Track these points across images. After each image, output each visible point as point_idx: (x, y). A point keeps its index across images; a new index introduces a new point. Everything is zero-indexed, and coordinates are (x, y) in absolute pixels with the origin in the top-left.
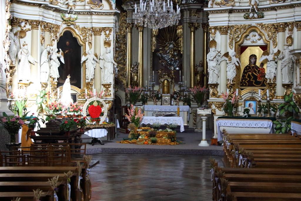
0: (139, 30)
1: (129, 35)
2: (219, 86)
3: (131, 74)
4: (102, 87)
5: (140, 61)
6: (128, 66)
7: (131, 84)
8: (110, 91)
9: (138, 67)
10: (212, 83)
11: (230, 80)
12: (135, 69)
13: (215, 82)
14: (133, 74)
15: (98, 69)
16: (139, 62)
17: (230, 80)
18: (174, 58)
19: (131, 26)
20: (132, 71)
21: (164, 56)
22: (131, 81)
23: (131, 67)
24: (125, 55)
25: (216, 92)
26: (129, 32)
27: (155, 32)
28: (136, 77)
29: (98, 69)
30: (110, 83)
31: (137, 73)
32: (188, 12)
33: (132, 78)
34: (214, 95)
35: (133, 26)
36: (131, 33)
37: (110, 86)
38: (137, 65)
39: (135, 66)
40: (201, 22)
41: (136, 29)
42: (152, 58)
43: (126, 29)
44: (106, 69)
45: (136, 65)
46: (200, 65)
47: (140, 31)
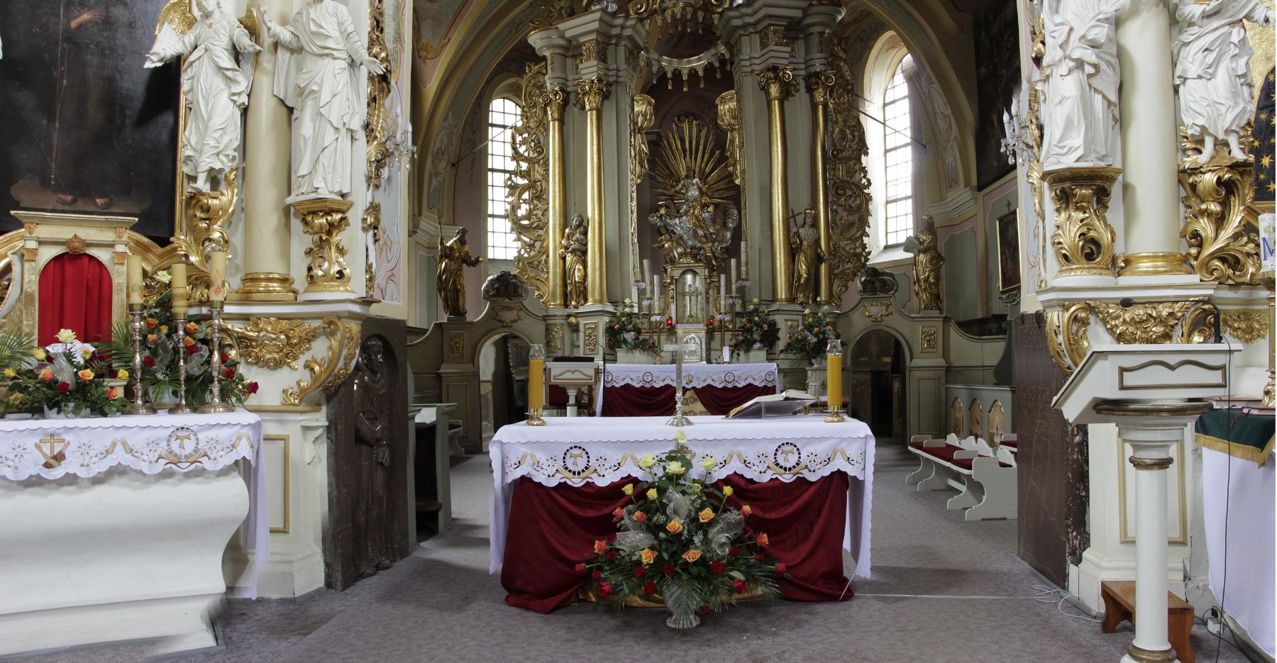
0: (587, 107)
1: (553, 129)
2: (1116, 190)
3: (564, 259)
4: (296, 224)
5: (592, 211)
6: (554, 232)
7: (565, 296)
8: (341, 251)
9: (585, 233)
10: (1082, 165)
11: (1209, 142)
12: (577, 240)
13: (1093, 155)
14: (569, 258)
15: (265, 111)
16: (589, 214)
17: (1209, 142)
18: (702, 228)
19: (559, 99)
20: (566, 248)
21: (672, 222)
22: (565, 285)
23: (563, 237)
24: (540, 196)
25: (1106, 238)
26: (554, 120)
27: (645, 115)
28: (579, 266)
29: (265, 111)
30: (343, 196)
31: (585, 253)
32: (756, 38)
33: (565, 275)
34: (1090, 257)
35: (566, 102)
36: (561, 121)
37: (337, 217)
38: (583, 226)
39: (575, 224)
40: (803, 73)
41: (576, 110)
42: (635, 203)
43: (545, 113)
44: (310, 103)
45: (578, 226)
46: (808, 220)
47: (591, 110)
